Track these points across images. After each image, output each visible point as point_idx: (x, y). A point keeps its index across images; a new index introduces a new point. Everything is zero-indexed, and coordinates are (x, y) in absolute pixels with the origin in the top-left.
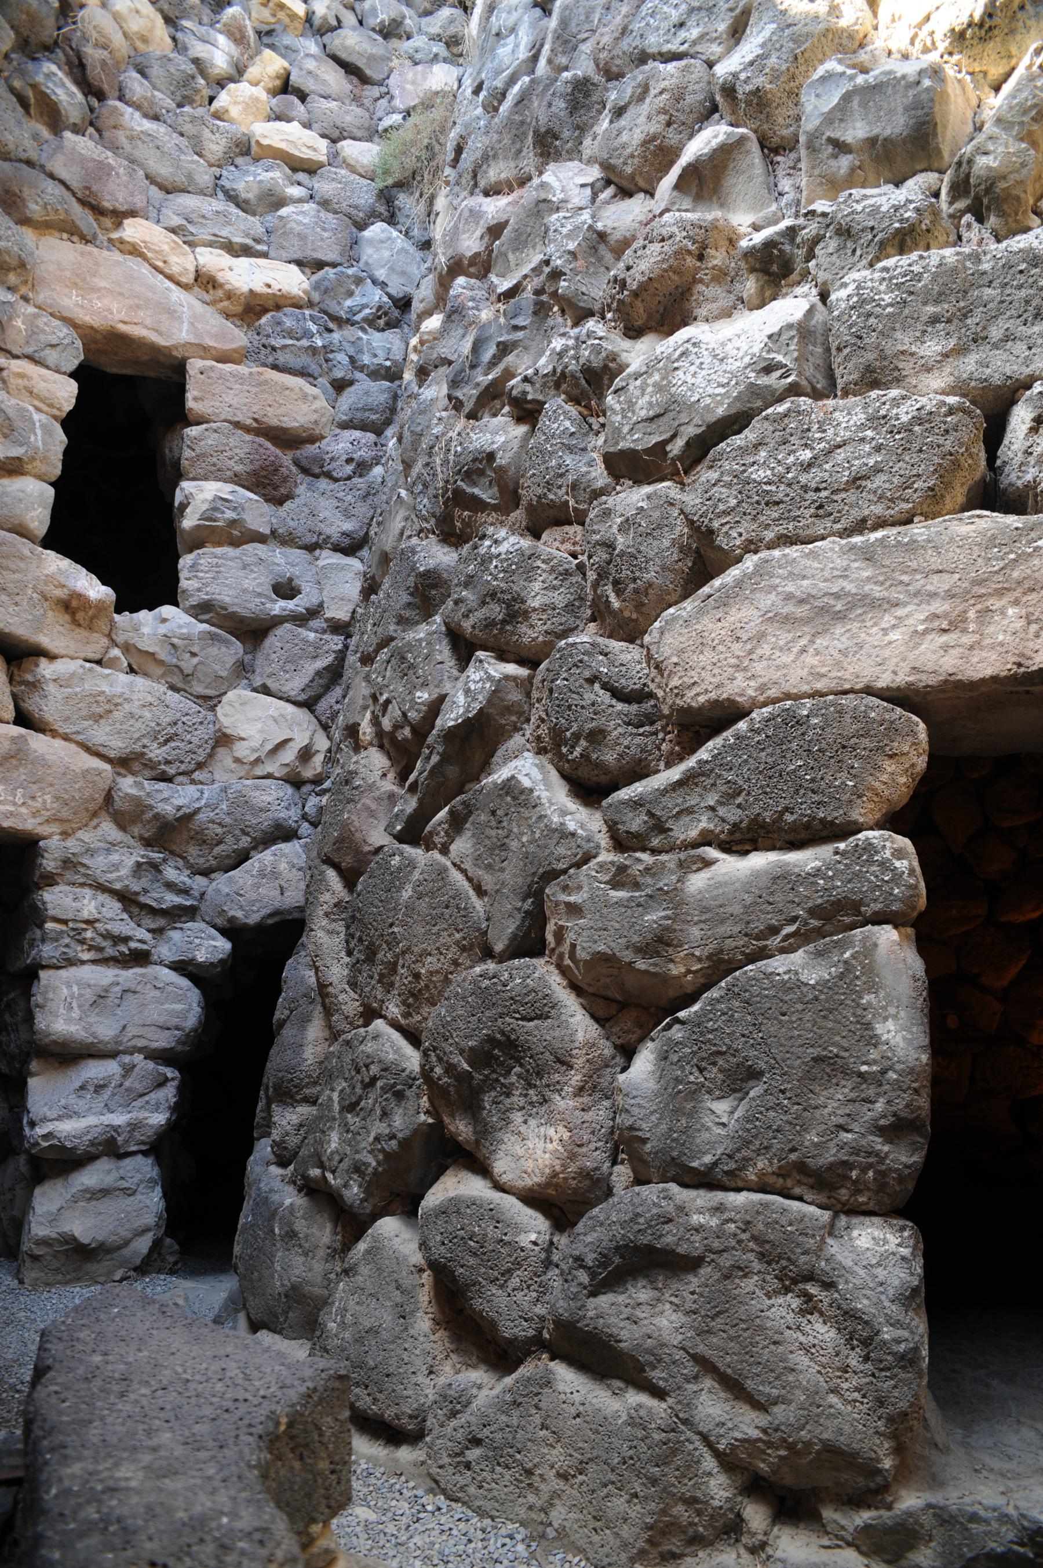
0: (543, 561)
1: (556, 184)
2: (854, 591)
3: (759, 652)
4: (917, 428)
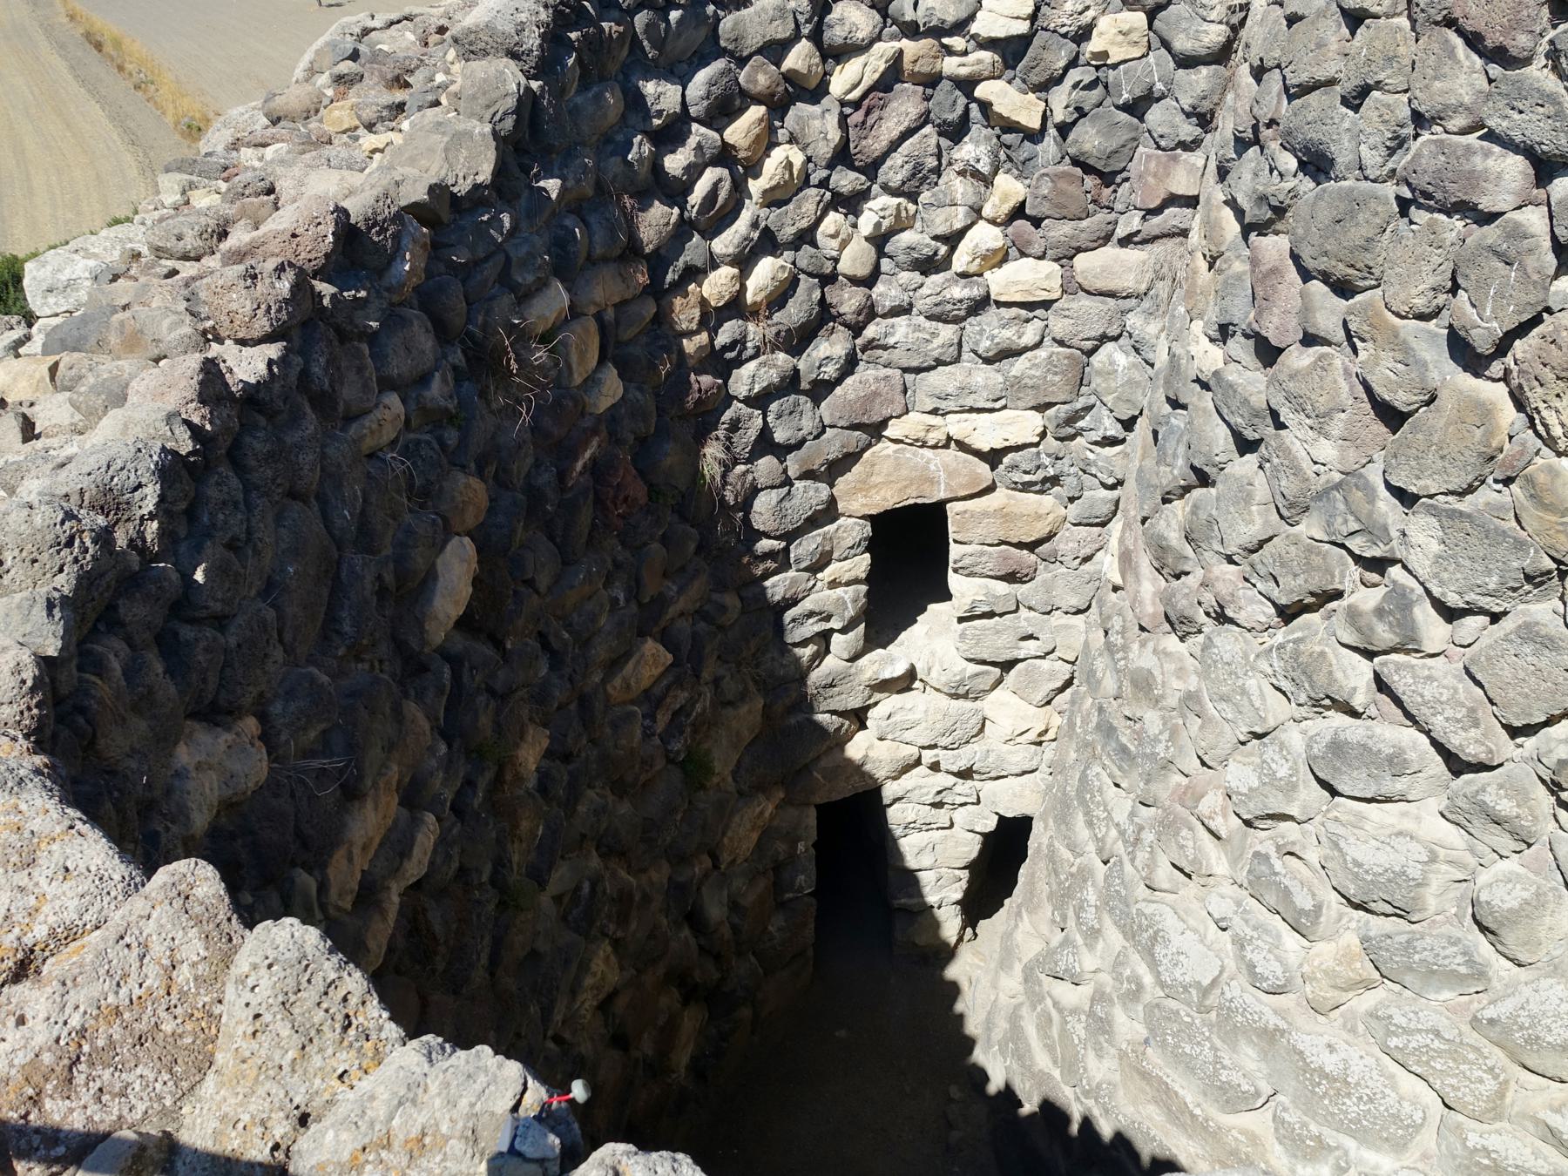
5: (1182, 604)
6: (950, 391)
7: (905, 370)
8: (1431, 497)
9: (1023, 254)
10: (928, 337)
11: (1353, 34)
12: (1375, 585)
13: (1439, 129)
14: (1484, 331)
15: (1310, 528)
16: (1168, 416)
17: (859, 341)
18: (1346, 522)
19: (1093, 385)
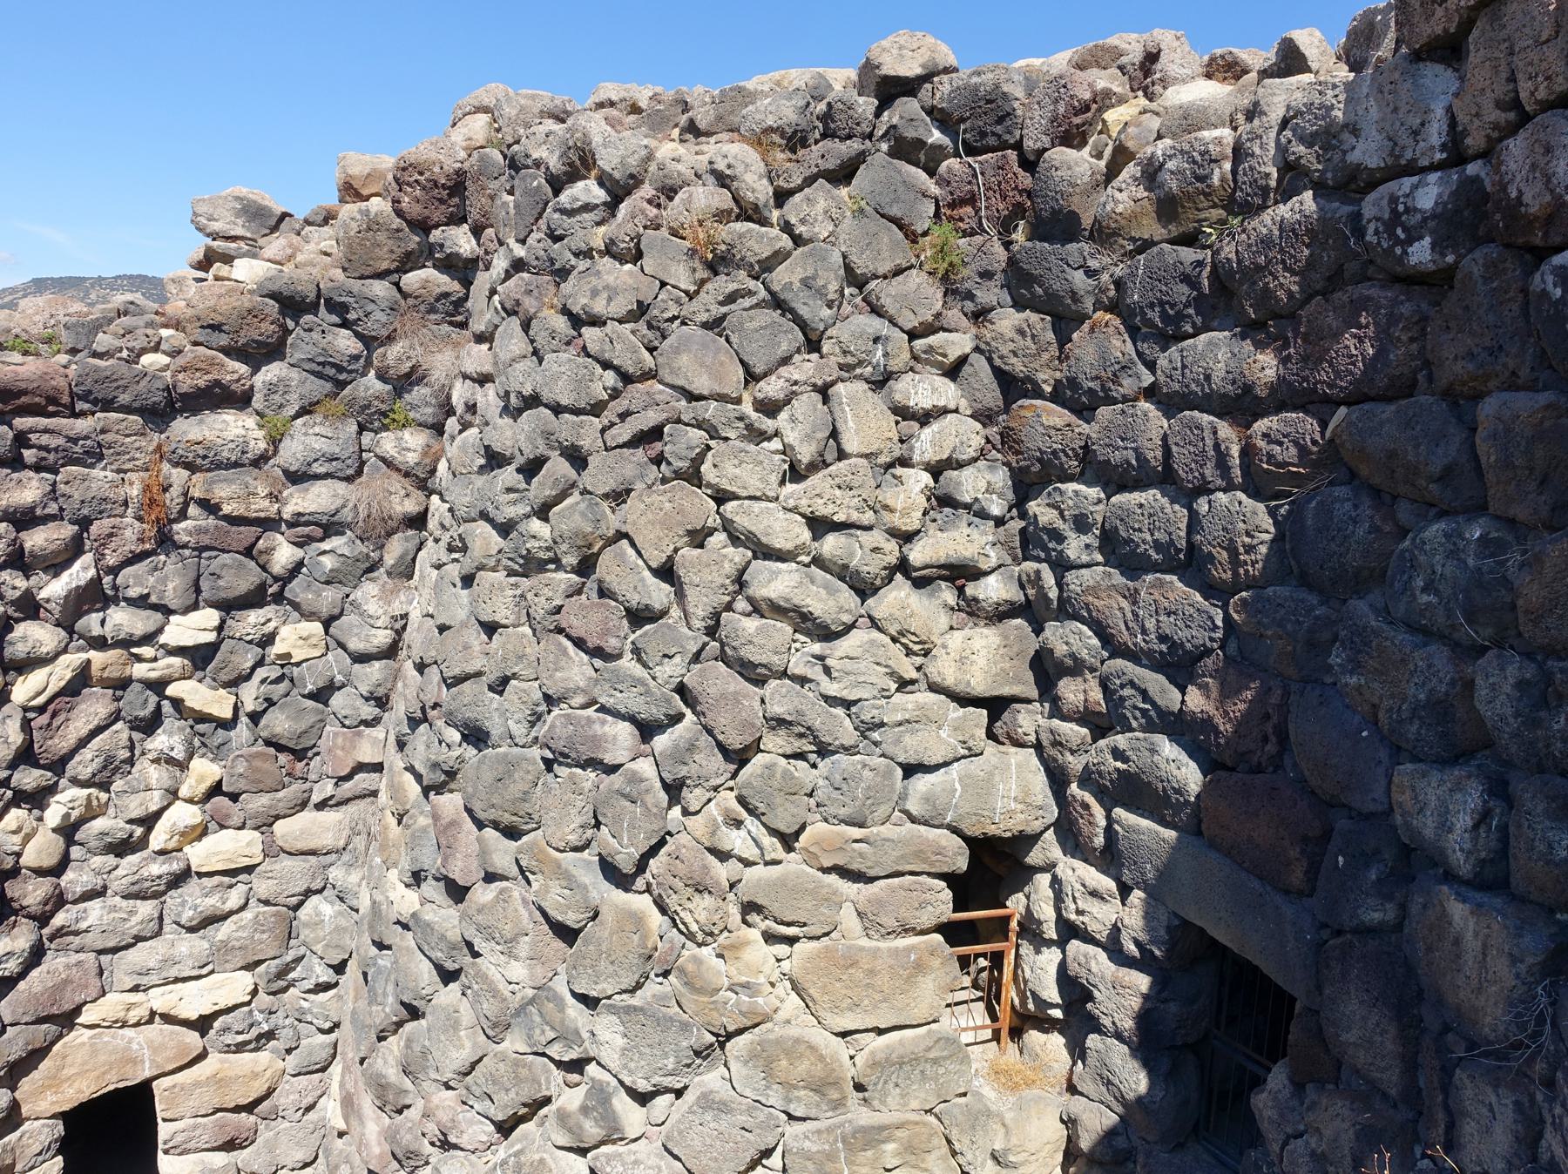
5: (406, 1139)
6: (151, 965)
7: (100, 952)
8: (609, 997)
9: (222, 827)
10: (125, 916)
11: (490, 638)
12: (577, 1085)
13: (565, 706)
14: (626, 859)
15: (513, 1043)
16: (374, 958)
17: (46, 931)
18: (543, 1032)
19: (302, 937)
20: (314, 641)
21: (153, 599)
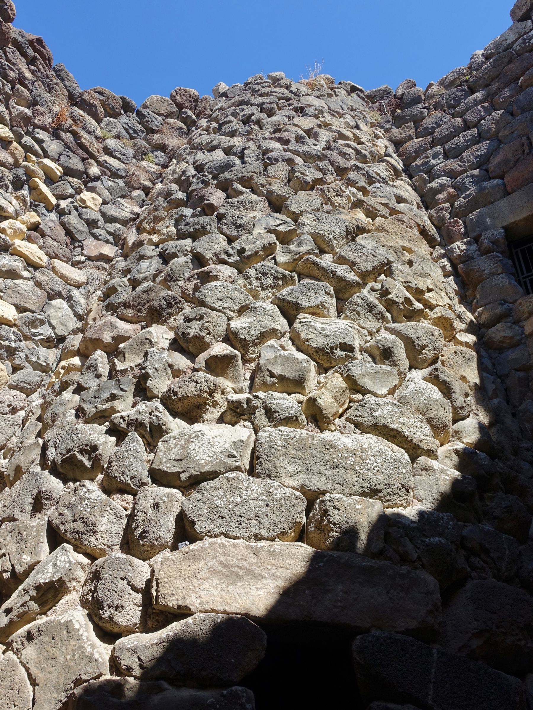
0: (111, 509)
1: (155, 334)
2: (248, 567)
3: (204, 586)
4: (283, 501)
20: (97, 202)
21: (44, 145)
